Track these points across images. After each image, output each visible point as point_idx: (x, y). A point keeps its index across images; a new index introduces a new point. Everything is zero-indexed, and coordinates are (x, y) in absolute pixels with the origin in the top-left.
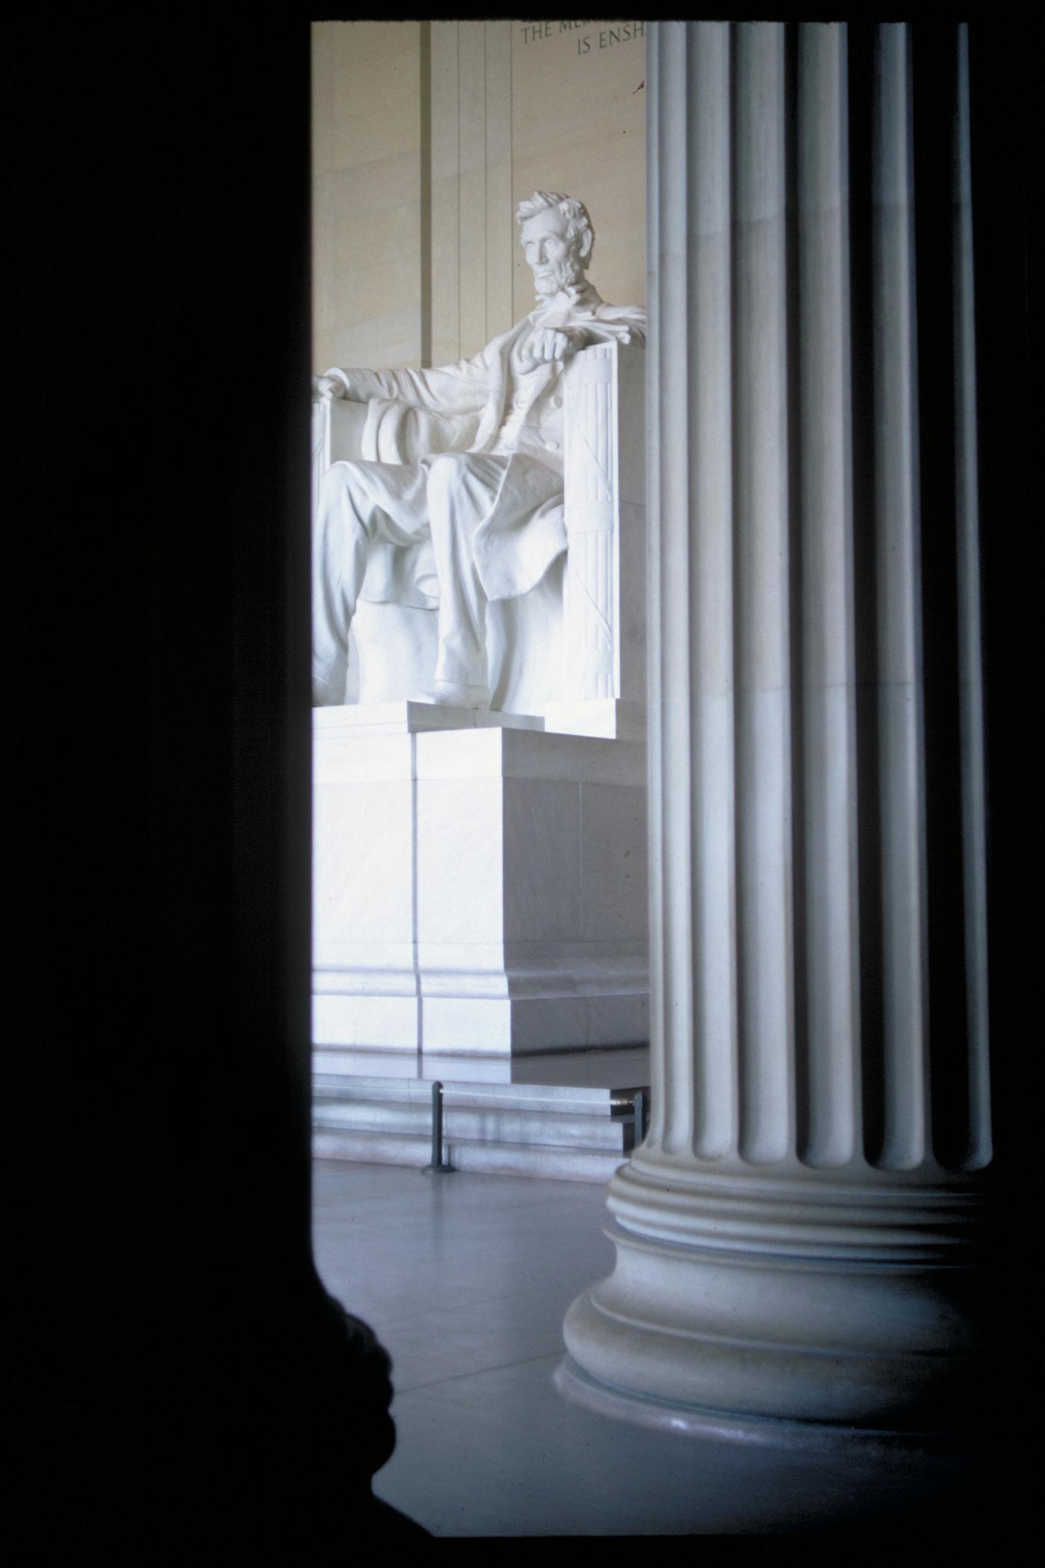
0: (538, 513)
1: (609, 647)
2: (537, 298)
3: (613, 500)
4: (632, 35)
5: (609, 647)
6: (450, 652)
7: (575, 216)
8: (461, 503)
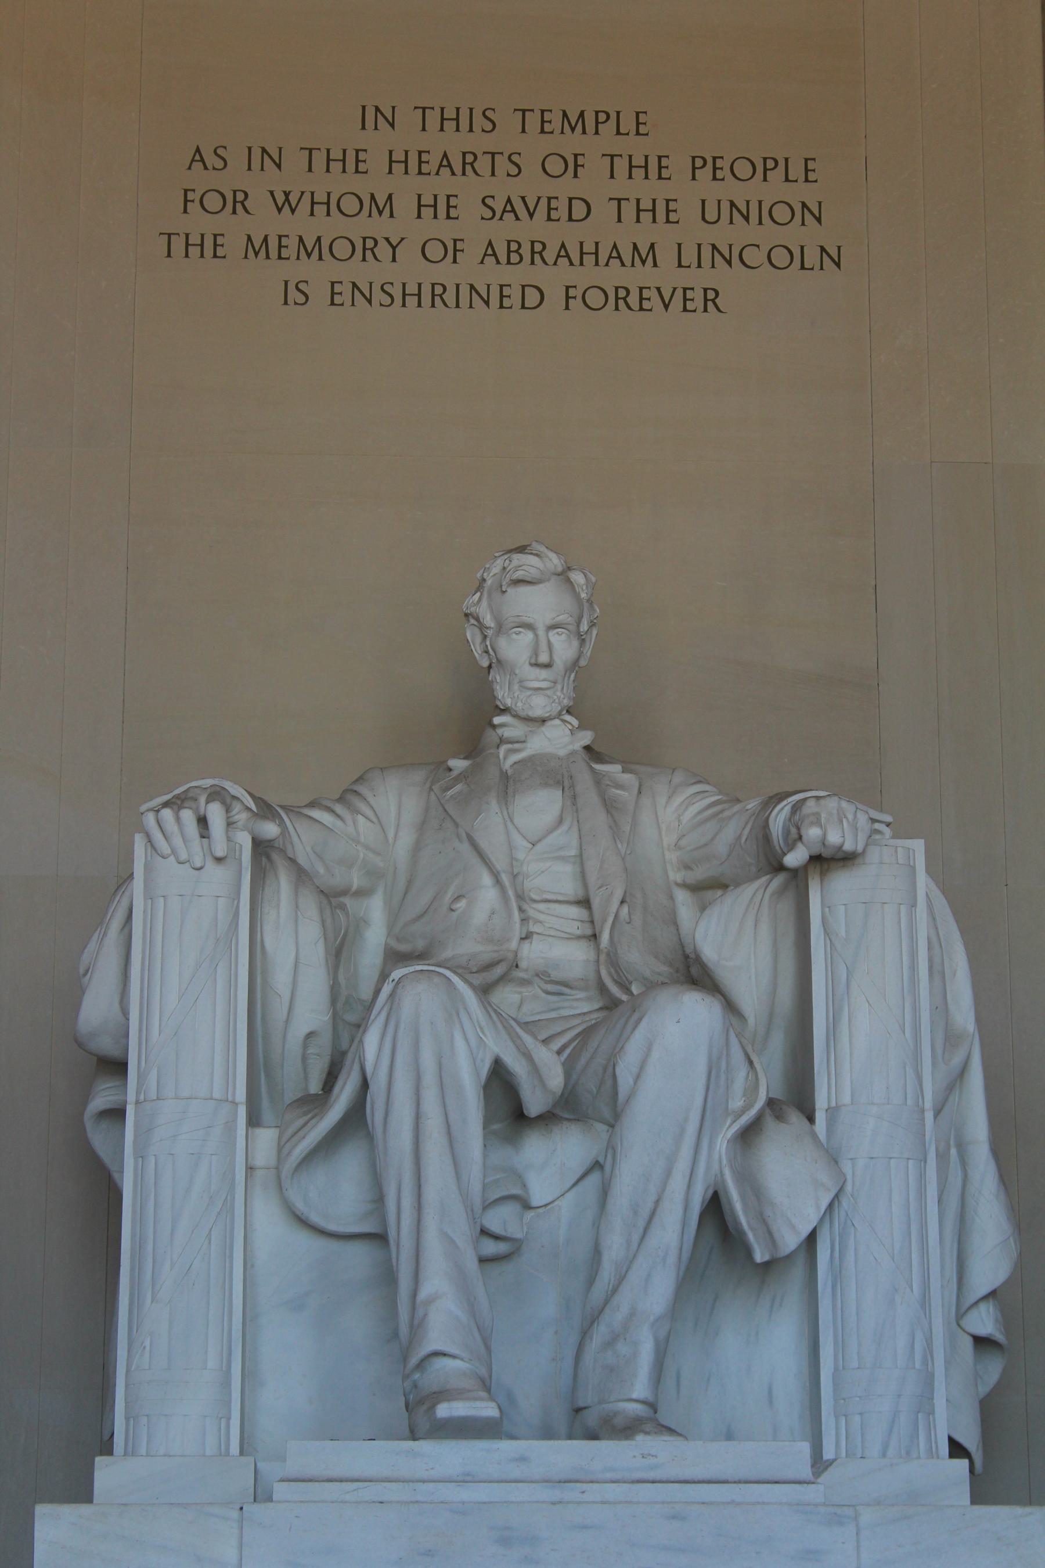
1: (930, 1363)
2: (497, 720)
3: (923, 1111)
5: (930, 1363)
7: (588, 601)
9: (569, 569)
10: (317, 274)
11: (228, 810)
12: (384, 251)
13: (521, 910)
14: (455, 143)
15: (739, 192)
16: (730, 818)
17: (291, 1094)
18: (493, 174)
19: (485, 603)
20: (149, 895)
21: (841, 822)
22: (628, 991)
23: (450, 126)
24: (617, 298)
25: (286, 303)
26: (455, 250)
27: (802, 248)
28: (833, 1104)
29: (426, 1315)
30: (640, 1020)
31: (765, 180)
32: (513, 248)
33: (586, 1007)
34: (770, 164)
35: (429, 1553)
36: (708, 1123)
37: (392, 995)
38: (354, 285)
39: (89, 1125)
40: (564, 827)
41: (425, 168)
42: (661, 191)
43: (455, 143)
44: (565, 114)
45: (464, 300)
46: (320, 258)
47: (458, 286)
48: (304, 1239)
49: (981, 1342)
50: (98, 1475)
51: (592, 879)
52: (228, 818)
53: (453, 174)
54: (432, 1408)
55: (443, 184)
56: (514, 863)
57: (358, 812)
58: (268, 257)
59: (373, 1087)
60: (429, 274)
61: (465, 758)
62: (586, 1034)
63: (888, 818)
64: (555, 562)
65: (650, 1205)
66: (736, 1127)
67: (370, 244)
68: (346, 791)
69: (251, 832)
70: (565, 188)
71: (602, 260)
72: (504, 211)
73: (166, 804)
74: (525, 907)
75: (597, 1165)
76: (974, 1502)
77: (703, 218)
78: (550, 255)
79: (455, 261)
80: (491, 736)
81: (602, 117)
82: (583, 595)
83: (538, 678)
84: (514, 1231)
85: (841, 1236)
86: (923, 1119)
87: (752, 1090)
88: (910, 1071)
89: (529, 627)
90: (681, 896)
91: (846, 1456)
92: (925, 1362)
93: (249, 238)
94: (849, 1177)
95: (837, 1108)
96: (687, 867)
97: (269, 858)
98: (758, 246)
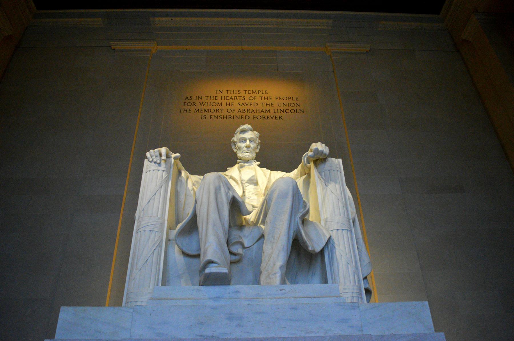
2: (238, 161)
6: (282, 275)
10: (208, 115)
12: (220, 111)
14: (233, 95)
15: (285, 102)
32: (244, 111)
35: (202, 323)
42: (270, 102)
60: (228, 114)
66: (301, 214)
70: (253, 101)
71: (260, 111)
78: (250, 111)
85: (331, 251)
88: (345, 209)
95: (327, 219)
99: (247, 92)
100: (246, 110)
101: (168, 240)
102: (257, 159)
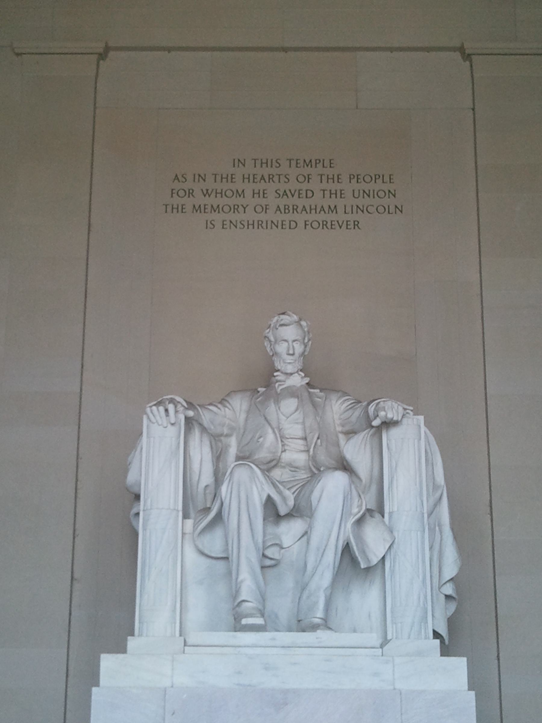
0: (367, 514)
2: (275, 374)
3: (423, 513)
4: (246, 227)
8: (347, 501)
9: (300, 320)
10: (218, 218)
11: (176, 407)
12: (241, 209)
13: (282, 441)
14: (266, 171)
15: (366, 187)
16: (357, 408)
17: (200, 506)
18: (279, 182)
19: (271, 333)
20: (148, 437)
21: (392, 409)
22: (319, 470)
23: (264, 165)
24: (323, 225)
25: (207, 228)
26: (266, 209)
27: (389, 206)
28: (391, 511)
29: (240, 587)
30: (320, 480)
31: (375, 182)
32: (286, 207)
33: (305, 476)
34: (377, 177)
35: (239, 673)
36: (344, 518)
37: (231, 473)
38: (231, 222)
39: (132, 518)
40: (298, 412)
41: (255, 180)
42: (339, 187)
43: (266, 171)
44: (305, 161)
45: (269, 227)
46: (219, 212)
47: (267, 222)
48: (203, 559)
49: (447, 597)
50: (128, 643)
51: (307, 431)
52: (175, 410)
53: (265, 182)
54: (241, 620)
55: (262, 186)
56: (280, 425)
57: (226, 407)
58: (201, 212)
59: (224, 504)
60: (257, 217)
61: (265, 387)
62: (303, 486)
63: (412, 408)
64: (295, 318)
65: (324, 547)
66: (354, 520)
67: (236, 207)
68: (223, 399)
69: (184, 414)
70: (305, 186)
71: (318, 212)
72: (283, 195)
73: (155, 405)
74: (283, 440)
75: (306, 533)
76: (441, 655)
77: (354, 196)
79: (266, 212)
80: (274, 379)
81: (318, 161)
82: (306, 329)
83: (289, 359)
84: (277, 556)
86: (423, 516)
87: (360, 506)
89: (286, 341)
90: (341, 436)
91: (396, 638)
92: (424, 605)
93: (194, 206)
94: (396, 536)
95: (392, 512)
96: (343, 426)
97: (192, 424)
98: (373, 206)
99: (293, 163)
100: (291, 208)
101: (183, 534)
102: (305, 370)
